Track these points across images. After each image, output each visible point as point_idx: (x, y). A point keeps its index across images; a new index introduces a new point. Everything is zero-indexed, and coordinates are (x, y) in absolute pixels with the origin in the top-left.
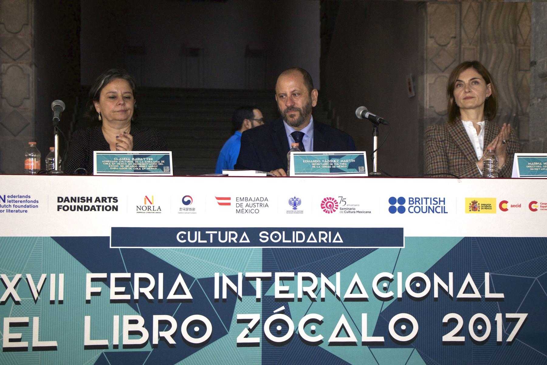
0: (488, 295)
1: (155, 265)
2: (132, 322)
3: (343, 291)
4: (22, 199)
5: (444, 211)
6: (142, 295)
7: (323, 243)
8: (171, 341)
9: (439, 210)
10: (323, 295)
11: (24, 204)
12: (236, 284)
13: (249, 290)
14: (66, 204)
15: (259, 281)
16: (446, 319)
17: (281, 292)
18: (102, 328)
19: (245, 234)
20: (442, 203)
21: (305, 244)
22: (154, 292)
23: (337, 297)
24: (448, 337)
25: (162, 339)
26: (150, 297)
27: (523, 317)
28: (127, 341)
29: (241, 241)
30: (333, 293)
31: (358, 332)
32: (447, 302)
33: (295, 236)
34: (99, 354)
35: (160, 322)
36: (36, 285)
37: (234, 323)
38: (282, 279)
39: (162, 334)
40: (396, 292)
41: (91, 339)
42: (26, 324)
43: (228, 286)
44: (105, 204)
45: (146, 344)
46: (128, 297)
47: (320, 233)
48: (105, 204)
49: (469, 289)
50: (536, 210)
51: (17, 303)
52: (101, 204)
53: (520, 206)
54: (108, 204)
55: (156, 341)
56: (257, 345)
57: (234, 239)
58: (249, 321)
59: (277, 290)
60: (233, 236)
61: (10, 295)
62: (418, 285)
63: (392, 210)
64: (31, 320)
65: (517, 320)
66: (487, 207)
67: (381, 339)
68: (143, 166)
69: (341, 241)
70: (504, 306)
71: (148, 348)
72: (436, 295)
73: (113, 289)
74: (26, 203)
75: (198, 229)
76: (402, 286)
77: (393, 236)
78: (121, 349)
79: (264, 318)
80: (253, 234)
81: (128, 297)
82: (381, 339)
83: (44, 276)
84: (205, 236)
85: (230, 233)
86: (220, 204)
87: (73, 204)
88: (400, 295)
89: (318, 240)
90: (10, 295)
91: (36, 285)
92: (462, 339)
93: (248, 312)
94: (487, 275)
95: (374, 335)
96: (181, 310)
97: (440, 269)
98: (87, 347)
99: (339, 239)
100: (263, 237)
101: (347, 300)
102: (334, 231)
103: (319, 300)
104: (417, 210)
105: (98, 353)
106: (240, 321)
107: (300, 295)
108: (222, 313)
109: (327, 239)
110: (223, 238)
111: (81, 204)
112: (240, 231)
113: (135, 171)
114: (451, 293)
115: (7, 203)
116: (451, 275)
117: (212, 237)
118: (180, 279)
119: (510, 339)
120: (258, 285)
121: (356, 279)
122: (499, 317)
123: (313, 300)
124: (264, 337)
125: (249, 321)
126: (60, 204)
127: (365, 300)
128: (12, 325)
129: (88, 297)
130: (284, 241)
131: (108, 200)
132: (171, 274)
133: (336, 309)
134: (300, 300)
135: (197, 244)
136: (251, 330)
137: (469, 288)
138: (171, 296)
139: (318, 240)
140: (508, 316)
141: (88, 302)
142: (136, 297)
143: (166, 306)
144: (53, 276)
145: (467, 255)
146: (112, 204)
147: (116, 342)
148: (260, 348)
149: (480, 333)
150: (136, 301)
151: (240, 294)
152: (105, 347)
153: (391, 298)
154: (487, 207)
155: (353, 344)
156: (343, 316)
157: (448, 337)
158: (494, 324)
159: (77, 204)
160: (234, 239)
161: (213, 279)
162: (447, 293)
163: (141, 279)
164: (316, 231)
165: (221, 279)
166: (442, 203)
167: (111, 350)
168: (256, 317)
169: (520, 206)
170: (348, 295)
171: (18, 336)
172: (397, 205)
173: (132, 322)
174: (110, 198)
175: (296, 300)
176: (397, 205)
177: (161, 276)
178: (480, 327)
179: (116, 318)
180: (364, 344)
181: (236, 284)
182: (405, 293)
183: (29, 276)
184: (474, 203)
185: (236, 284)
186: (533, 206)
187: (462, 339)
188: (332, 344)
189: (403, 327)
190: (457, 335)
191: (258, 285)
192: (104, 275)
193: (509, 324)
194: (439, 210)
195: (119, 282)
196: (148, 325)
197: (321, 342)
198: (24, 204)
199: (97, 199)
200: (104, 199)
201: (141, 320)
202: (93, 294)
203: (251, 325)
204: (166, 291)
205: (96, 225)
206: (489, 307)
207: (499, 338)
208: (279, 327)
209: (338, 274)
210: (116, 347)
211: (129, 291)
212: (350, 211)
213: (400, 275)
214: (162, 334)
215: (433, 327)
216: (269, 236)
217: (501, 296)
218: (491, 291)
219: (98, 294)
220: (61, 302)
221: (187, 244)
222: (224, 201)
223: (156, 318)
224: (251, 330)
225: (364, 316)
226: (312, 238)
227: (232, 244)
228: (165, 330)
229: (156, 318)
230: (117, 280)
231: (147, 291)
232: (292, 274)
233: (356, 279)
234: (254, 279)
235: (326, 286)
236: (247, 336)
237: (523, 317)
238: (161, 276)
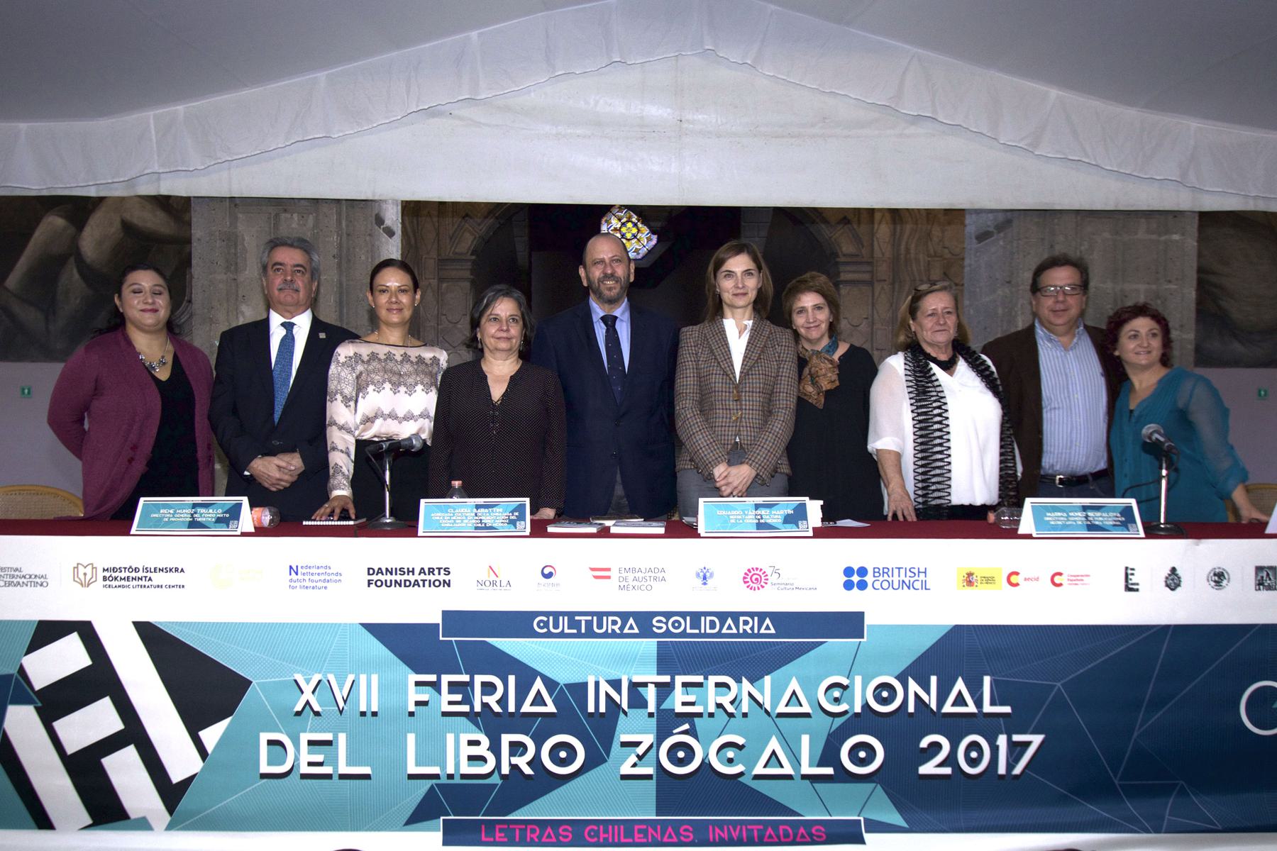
0: (988, 708)
1: (505, 665)
2: (471, 743)
3: (775, 703)
4: (321, 571)
5: (925, 586)
6: (485, 706)
7: (745, 634)
8: (528, 771)
9: (918, 585)
10: (745, 709)
11: (322, 577)
12: (619, 692)
13: (637, 701)
14: (378, 577)
15: (652, 688)
16: (924, 743)
17: (684, 704)
18: (432, 749)
19: (631, 621)
20: (922, 575)
21: (719, 635)
22: (503, 701)
23: (766, 711)
24: (928, 769)
25: (514, 768)
26: (497, 709)
27: (1037, 740)
28: (466, 769)
29: (626, 631)
30: (760, 705)
31: (796, 761)
32: (927, 719)
33: (705, 622)
34: (428, 786)
35: (512, 744)
36: (341, 690)
37: (616, 746)
38: (685, 685)
39: (515, 760)
40: (852, 704)
41: (417, 765)
42: (329, 743)
43: (607, 694)
44: (432, 578)
45: (492, 772)
46: (466, 708)
47: (742, 619)
48: (432, 578)
49: (960, 701)
50: (1060, 585)
51: (317, 714)
52: (427, 577)
53: (1037, 579)
54: (438, 577)
55: (505, 770)
56: (649, 777)
57: (616, 628)
58: (637, 744)
59: (678, 701)
60: (614, 623)
61: (308, 703)
62: (885, 694)
63: (848, 586)
64: (336, 737)
65: (1028, 744)
66: (989, 580)
67: (829, 771)
69: (773, 631)
70: (1010, 724)
71: (495, 779)
72: (911, 709)
73: (446, 696)
74: (326, 577)
75: (564, 614)
76: (861, 695)
77: (850, 624)
78: (457, 780)
79: (660, 739)
80: (644, 622)
81: (466, 708)
82: (829, 771)
83: (351, 678)
84: (574, 624)
85: (611, 618)
86: (596, 577)
87: (389, 577)
88: (858, 709)
89: (738, 629)
90: (308, 703)
91: (341, 690)
92: (947, 771)
93: (636, 730)
94: (987, 680)
95: (820, 765)
96: (541, 727)
97: (918, 671)
98: (411, 777)
99: (768, 627)
100: (658, 625)
101: (780, 715)
102: (762, 616)
103: (739, 716)
104: (885, 585)
105: (428, 784)
106: (625, 744)
107: (712, 709)
108: (599, 732)
109: (752, 628)
110: (600, 626)
111: (399, 578)
112: (624, 616)
113: (477, 528)
114: (934, 706)
115: (300, 577)
116: (934, 679)
117: (582, 625)
118: (539, 685)
119: (1017, 770)
120: (651, 694)
121: (794, 685)
122: (1002, 741)
123: (731, 715)
124: (659, 766)
125: (637, 744)
126: (371, 577)
127: (807, 715)
128: (311, 743)
129: (412, 708)
130: (689, 631)
131: (436, 572)
132: (526, 676)
133: (762, 730)
134: (711, 715)
135: (562, 635)
136: (640, 757)
137: (960, 698)
138: (527, 708)
139: (738, 629)
140: (1016, 738)
141: (412, 714)
142: (478, 708)
143: (519, 722)
144: (363, 678)
145: (959, 651)
146: (442, 577)
147: (450, 770)
148: (654, 782)
149: (973, 763)
150: (478, 714)
151: (625, 705)
152: (437, 776)
153: (846, 712)
154: (989, 580)
155: (789, 777)
156: (774, 738)
157: (928, 769)
158: (995, 750)
159: (394, 577)
160: (616, 628)
161: (585, 685)
162: (927, 706)
163: (484, 684)
164: (735, 616)
165: (597, 684)
166: (922, 575)
167: (444, 780)
168: (648, 739)
169: (1037, 579)
170: (782, 708)
171: (319, 758)
172: (856, 579)
173: (471, 743)
174: (439, 569)
175: (706, 715)
176: (855, 578)
177: (512, 679)
178: (974, 755)
179: (450, 738)
180: (804, 777)
181: (619, 692)
182: (866, 706)
183: (332, 678)
184: (970, 575)
185: (619, 692)
186: (1057, 579)
187: (947, 771)
188: (757, 777)
189: (862, 754)
190: (941, 765)
191: (651, 694)
192: (433, 678)
193: (1017, 750)
194: (918, 585)
195: (453, 687)
196: (495, 748)
197: (741, 774)
198: (322, 577)
199: (422, 571)
200: (431, 571)
201: (485, 742)
202: (418, 703)
203: (640, 750)
204: (520, 702)
205: (423, 608)
206: (989, 726)
207: (1002, 770)
208: (682, 753)
209: (767, 679)
210: (450, 776)
211: (467, 700)
212: (787, 586)
213: (858, 680)
214: (515, 760)
215: (905, 754)
216: (666, 624)
217: (1007, 709)
218: (993, 703)
219: (425, 703)
220: (375, 714)
221: (549, 635)
222: (601, 573)
223: (506, 739)
224: (640, 757)
225: (805, 739)
226: (729, 627)
227: (614, 635)
228: (520, 755)
229: (506, 739)
230: (450, 684)
231: (492, 700)
232: (699, 679)
233: (794, 685)
234: (645, 685)
235: (750, 694)
236: (635, 765)
237: (1037, 740)
238: (512, 679)
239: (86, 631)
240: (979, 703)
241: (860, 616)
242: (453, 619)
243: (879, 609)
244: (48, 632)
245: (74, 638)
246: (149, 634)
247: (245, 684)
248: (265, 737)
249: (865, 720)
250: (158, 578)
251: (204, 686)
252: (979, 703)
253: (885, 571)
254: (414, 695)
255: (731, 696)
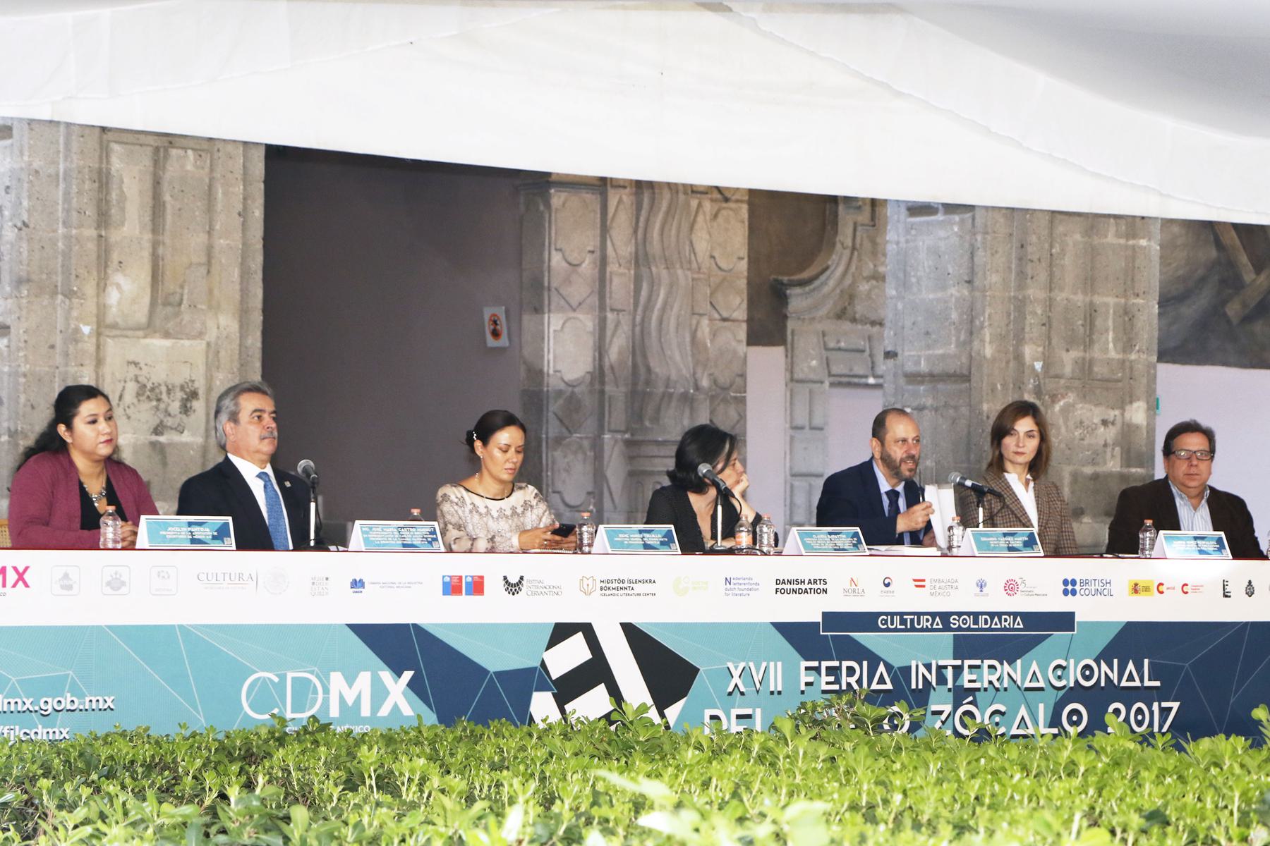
0: (1147, 683)
7: (1005, 629)
13: (942, 680)
15: (950, 669)
17: (970, 681)
26: (856, 686)
27: (1175, 705)
32: (1111, 692)
33: (982, 619)
38: (970, 667)
40: (1068, 680)
44: (816, 587)
46: (836, 687)
48: (816, 587)
51: (742, 694)
66: (1147, 589)
67: (1055, 731)
68: (841, 545)
72: (1103, 684)
73: (825, 678)
76: (1074, 675)
77: (1064, 621)
79: (955, 709)
81: (836, 687)
83: (764, 665)
84: (903, 622)
87: (789, 586)
94: (1146, 662)
97: (1105, 656)
100: (955, 622)
101: (1027, 689)
102: (1015, 615)
107: (986, 685)
116: (1116, 661)
117: (908, 622)
120: (949, 673)
121: (1034, 667)
122: (1155, 706)
123: (997, 690)
125: (941, 713)
127: (1041, 689)
129: (803, 687)
132: (874, 661)
134: (986, 689)
135: (896, 630)
136: (943, 723)
140: (1164, 705)
141: (803, 692)
142: (844, 687)
144: (772, 664)
145: (1133, 640)
146: (822, 586)
151: (934, 683)
154: (1147, 589)
158: (1152, 713)
161: (910, 667)
164: (999, 615)
168: (948, 708)
170: (1028, 684)
176: (1070, 587)
177: (865, 663)
182: (1077, 682)
183: (751, 665)
191: (949, 673)
192: (816, 664)
193: (1165, 712)
195: (830, 671)
202: (808, 684)
203: (943, 717)
205: (808, 610)
209: (1019, 662)
211: (837, 681)
212: (1029, 593)
213: (1072, 661)
220: (779, 693)
221: (888, 630)
222: (920, 583)
224: (943, 723)
225: (1041, 706)
227: (927, 630)
230: (827, 668)
231: (853, 680)
232: (978, 662)
233: (1034, 667)
234: (946, 667)
237: (1175, 705)
239: (587, 630)
240: (1142, 680)
241: (1071, 615)
242: (831, 619)
243: (1085, 609)
244: (561, 632)
245: (579, 638)
246: (630, 630)
247: (694, 671)
248: (708, 712)
249: (1075, 693)
250: (639, 588)
251: (668, 673)
252: (1142, 680)
253: (1087, 582)
254: (805, 678)
255: (997, 675)
